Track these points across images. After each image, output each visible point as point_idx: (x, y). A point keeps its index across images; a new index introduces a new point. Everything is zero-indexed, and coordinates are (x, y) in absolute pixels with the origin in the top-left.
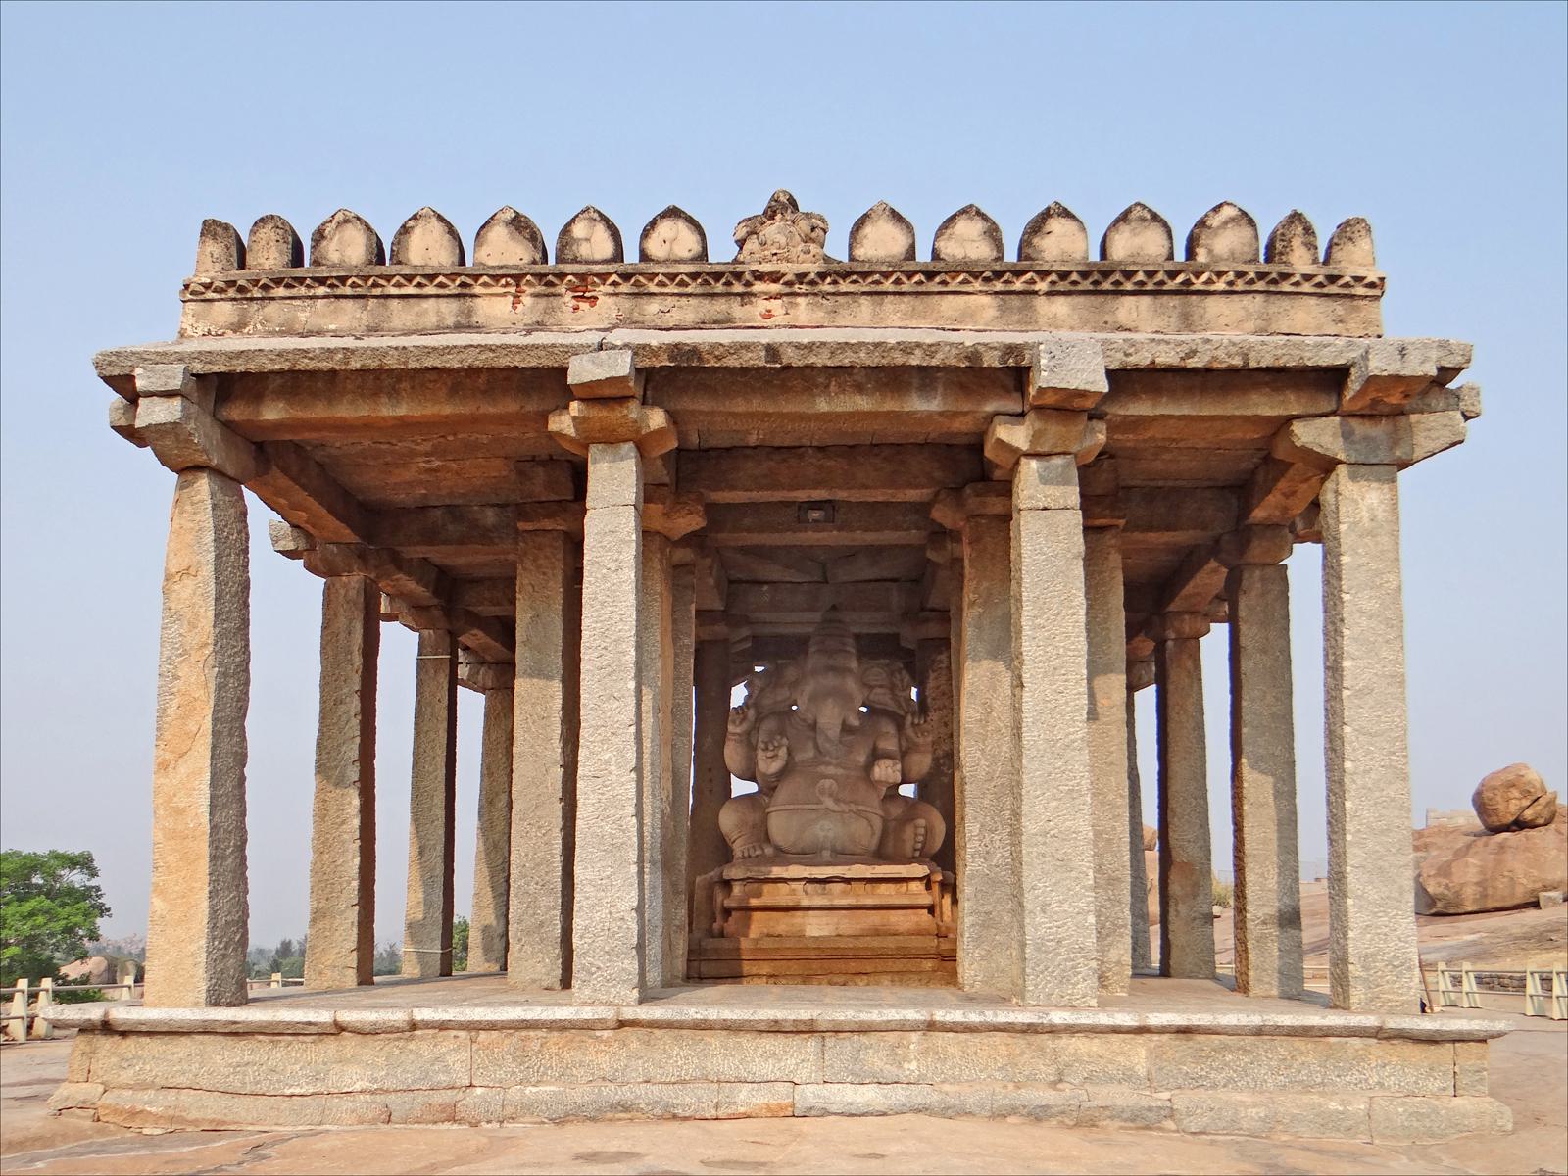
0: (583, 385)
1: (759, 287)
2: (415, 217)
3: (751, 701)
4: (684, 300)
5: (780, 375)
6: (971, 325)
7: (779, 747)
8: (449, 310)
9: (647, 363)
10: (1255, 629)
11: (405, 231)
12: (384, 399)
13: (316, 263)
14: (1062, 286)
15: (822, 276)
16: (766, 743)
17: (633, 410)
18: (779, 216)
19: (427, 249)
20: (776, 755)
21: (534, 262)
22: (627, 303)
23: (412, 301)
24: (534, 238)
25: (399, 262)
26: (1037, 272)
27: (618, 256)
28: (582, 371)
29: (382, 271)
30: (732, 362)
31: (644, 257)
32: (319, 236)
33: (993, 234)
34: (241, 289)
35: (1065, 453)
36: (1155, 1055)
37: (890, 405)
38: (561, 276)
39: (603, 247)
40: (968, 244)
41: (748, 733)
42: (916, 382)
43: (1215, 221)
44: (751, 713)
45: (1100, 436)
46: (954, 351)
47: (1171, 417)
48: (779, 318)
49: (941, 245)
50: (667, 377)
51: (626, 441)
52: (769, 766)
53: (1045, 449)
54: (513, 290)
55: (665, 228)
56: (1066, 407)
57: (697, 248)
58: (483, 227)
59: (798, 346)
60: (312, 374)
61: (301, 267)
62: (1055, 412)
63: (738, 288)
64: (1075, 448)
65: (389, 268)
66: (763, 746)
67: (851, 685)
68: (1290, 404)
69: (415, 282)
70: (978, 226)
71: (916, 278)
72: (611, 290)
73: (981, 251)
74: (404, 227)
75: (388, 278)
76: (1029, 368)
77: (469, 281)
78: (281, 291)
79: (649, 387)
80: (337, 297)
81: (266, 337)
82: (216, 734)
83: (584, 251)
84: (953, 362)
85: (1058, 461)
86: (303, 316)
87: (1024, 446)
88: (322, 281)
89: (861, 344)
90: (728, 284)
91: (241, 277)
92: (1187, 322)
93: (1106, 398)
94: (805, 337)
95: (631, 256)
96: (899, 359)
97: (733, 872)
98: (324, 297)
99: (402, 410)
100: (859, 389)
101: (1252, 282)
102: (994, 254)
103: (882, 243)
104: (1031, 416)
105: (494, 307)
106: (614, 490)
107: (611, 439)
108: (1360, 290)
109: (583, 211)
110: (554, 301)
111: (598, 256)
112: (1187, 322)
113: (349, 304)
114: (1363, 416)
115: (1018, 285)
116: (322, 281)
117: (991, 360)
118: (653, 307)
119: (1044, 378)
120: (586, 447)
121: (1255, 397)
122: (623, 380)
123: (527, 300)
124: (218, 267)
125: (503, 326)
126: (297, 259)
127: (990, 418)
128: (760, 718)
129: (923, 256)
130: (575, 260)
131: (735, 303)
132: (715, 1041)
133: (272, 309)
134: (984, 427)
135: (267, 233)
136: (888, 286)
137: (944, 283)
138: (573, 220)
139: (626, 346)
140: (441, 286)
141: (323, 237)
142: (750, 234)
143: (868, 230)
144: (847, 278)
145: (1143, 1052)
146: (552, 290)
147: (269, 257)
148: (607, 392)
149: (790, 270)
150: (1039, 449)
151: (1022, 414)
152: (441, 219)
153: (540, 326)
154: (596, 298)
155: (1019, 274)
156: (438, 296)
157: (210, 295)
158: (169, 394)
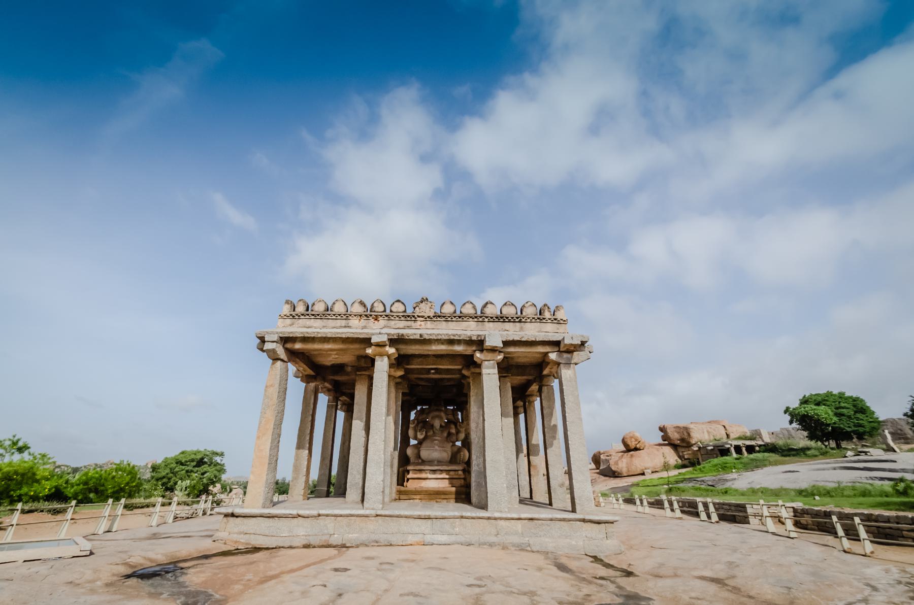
5: (423, 341)
6: (470, 330)
8: (343, 323)
17: (387, 348)
19: (339, 308)
27: (385, 311)
28: (374, 340)
29: (328, 313)
30: (411, 337)
31: (391, 311)
32: (314, 304)
33: (474, 307)
39: (381, 308)
40: (468, 310)
45: (500, 357)
48: (423, 326)
50: (394, 341)
52: (420, 436)
55: (396, 304)
56: (493, 350)
60: (308, 338)
61: (309, 312)
65: (329, 312)
73: (472, 311)
81: (299, 328)
83: (377, 309)
91: (294, 314)
92: (521, 329)
94: (429, 332)
96: (452, 337)
97: (409, 468)
100: (443, 344)
103: (448, 309)
105: (354, 322)
106: (382, 367)
107: (381, 355)
117: (474, 338)
118: (392, 323)
119: (489, 343)
126: (307, 310)
128: (418, 423)
129: (458, 313)
132: (402, 520)
135: (301, 303)
147: (300, 309)
153: (365, 327)
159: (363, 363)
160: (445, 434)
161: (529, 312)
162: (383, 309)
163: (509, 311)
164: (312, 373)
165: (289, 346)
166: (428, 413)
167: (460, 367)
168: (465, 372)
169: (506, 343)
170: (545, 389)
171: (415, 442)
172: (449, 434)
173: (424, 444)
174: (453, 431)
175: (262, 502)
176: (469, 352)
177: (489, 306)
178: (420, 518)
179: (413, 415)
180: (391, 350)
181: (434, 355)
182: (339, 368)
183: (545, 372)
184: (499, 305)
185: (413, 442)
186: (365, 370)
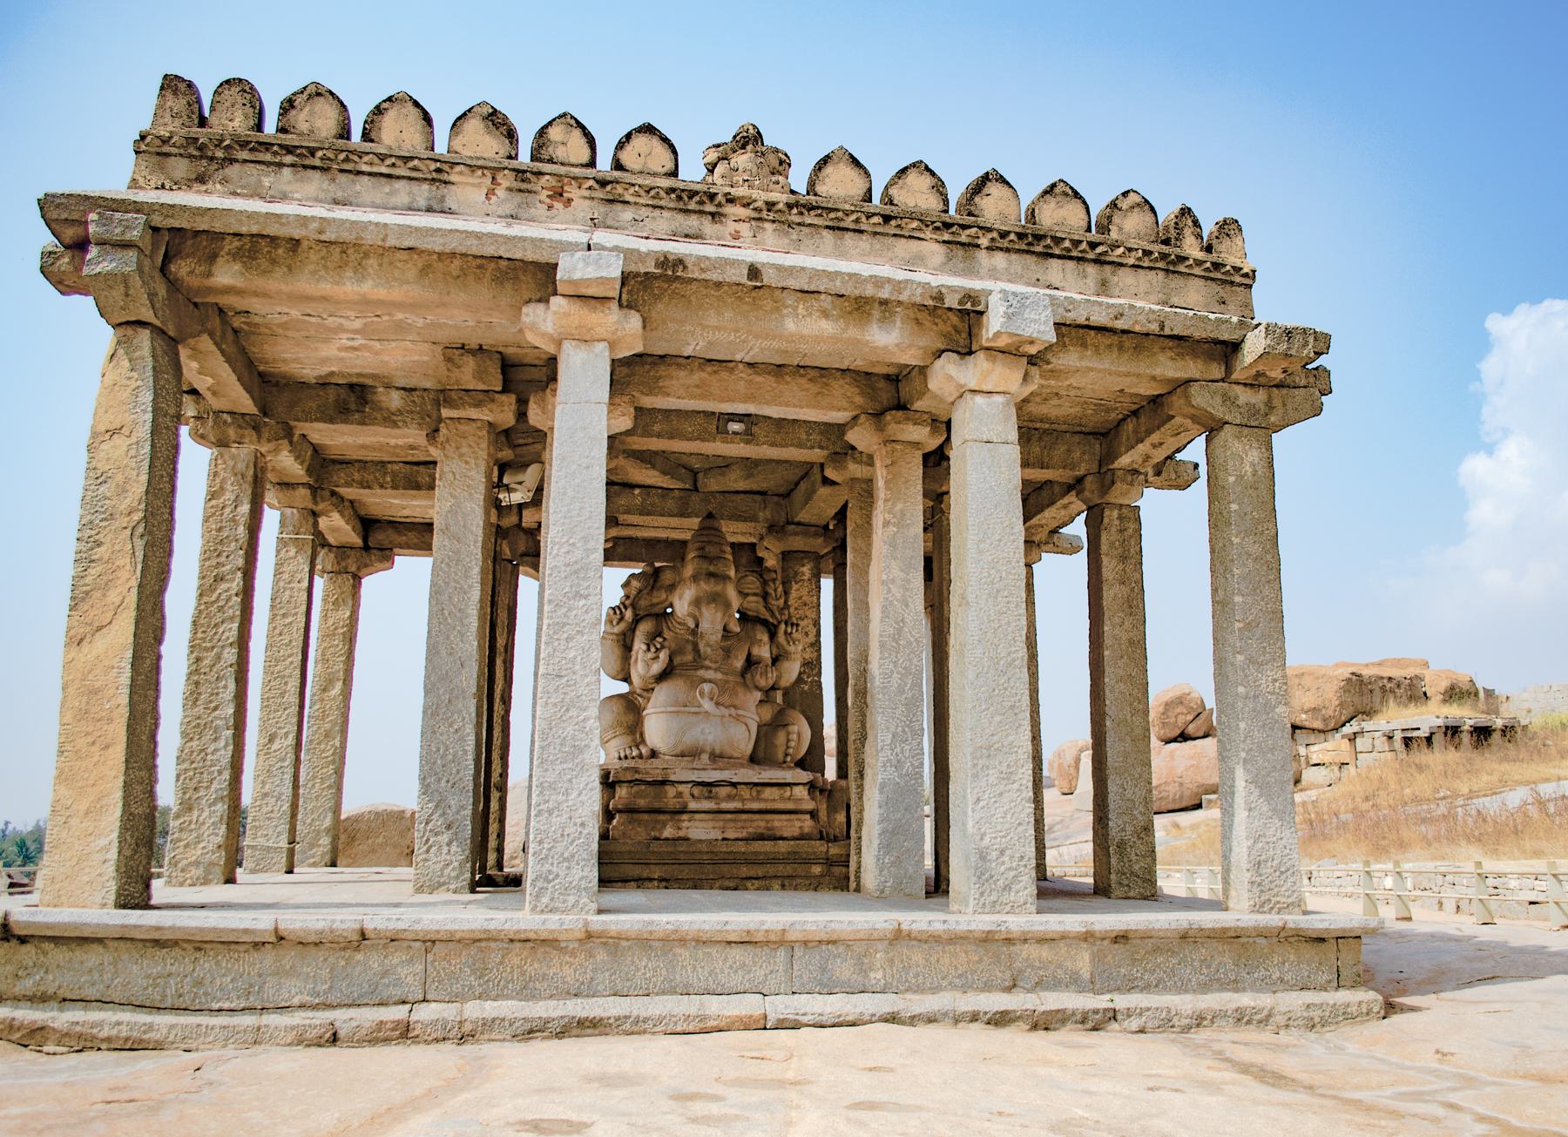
0: (571, 282)
1: (729, 209)
2: (390, 99)
4: (657, 212)
7: (663, 647)
8: (423, 192)
9: (633, 268)
10: (1114, 562)
11: (378, 111)
12: (349, 274)
13: (282, 130)
14: (1005, 243)
15: (790, 206)
18: (749, 147)
21: (510, 157)
22: (599, 211)
23: (383, 180)
24: (511, 135)
25: (372, 141)
26: (981, 228)
27: (592, 164)
30: (714, 276)
31: (618, 165)
32: (288, 105)
34: (201, 148)
36: (1097, 958)
37: (853, 332)
38: (540, 174)
39: (576, 150)
40: (915, 195)
41: (624, 634)
42: (876, 313)
43: (1124, 204)
44: (629, 614)
46: (919, 290)
47: (1092, 369)
49: (893, 191)
50: (644, 287)
53: (989, 388)
54: (488, 181)
55: (640, 142)
57: (670, 166)
58: (459, 118)
59: (779, 268)
63: (710, 208)
66: (644, 647)
68: (1191, 368)
69: (389, 161)
70: (927, 180)
71: (876, 220)
72: (587, 193)
73: (930, 203)
74: (377, 107)
75: (361, 155)
76: (981, 313)
77: (446, 167)
78: (244, 155)
79: (625, 290)
80: (305, 167)
82: (139, 608)
83: (560, 153)
84: (918, 300)
85: (999, 399)
86: (266, 182)
87: (973, 385)
88: (289, 150)
89: (837, 273)
90: (701, 203)
91: (202, 134)
93: (1050, 348)
95: (604, 163)
96: (869, 291)
98: (293, 165)
99: (367, 288)
100: (825, 314)
101: (1156, 260)
102: (941, 207)
104: (981, 355)
107: (585, 340)
108: (1238, 279)
109: (560, 117)
110: (530, 197)
111: (573, 161)
112: (1104, 287)
113: (317, 175)
114: (1245, 385)
115: (963, 239)
116: (289, 150)
117: (952, 301)
118: (627, 214)
120: (559, 344)
121: (1162, 358)
122: (614, 279)
123: (500, 192)
124: (178, 122)
125: (478, 218)
126: (259, 127)
128: (637, 620)
130: (551, 161)
131: (707, 220)
133: (233, 171)
135: (232, 93)
136: (848, 222)
137: (898, 226)
138: (550, 123)
139: (616, 248)
140: (415, 169)
141: (293, 107)
142: (719, 159)
143: (829, 170)
144: (807, 213)
145: (1087, 956)
146: (524, 186)
148: (589, 292)
149: (761, 197)
150: (985, 388)
151: (970, 353)
152: (416, 104)
154: (570, 201)
155: (964, 227)
156: (410, 179)
157: (166, 149)
158: (126, 245)
159: (467, 375)
160: (739, 663)
161: (1131, 226)
162: (585, 156)
163: (1059, 218)
164: (247, 404)
165: (182, 269)
166: (672, 588)
169: (1071, 331)
170: (1111, 515)
172: (750, 662)
173: (662, 693)
174: (764, 652)
175: (113, 887)
176: (910, 358)
177: (994, 189)
180: (634, 321)
181: (750, 365)
182: (353, 398)
183: (1125, 461)
184: (1028, 192)
186: (478, 404)
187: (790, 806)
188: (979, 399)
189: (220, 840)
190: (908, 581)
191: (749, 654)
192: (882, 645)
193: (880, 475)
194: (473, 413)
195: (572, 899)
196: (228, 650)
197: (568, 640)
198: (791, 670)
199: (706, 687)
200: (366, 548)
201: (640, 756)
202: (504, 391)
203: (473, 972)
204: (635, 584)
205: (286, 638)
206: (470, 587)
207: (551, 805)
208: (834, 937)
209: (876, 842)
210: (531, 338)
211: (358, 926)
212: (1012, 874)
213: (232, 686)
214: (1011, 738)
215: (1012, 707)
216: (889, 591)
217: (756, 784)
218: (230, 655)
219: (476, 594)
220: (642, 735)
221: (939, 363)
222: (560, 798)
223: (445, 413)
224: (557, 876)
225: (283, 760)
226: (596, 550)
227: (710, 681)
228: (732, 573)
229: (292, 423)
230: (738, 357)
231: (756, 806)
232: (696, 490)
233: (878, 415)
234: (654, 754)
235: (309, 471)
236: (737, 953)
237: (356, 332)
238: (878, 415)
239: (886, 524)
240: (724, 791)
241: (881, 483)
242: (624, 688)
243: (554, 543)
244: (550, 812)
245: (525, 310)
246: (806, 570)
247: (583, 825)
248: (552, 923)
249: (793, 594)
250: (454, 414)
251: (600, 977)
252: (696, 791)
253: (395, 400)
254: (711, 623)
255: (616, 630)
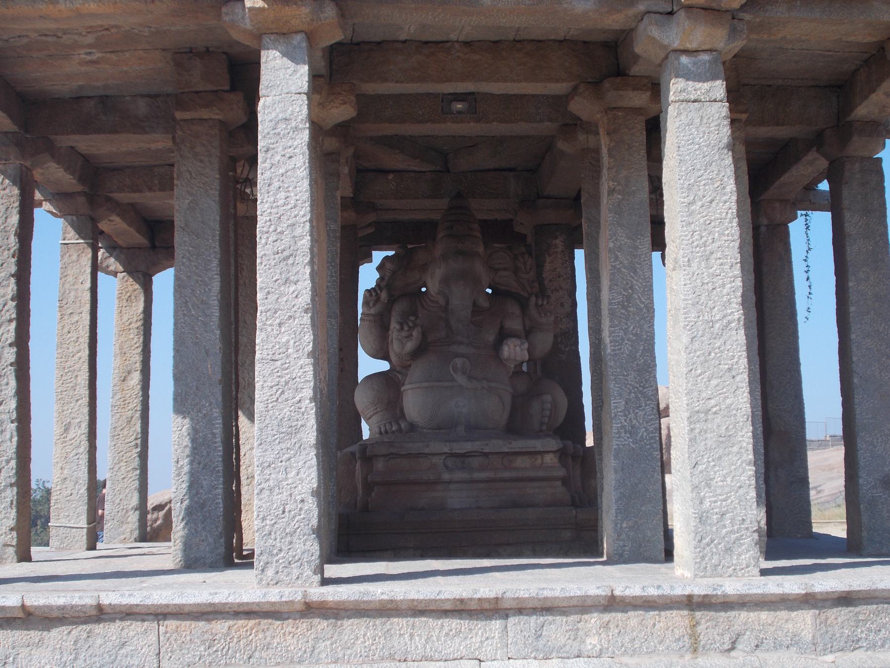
3: (383, 284)
7: (415, 326)
16: (401, 324)
20: (412, 335)
35: (711, 50)
44: (384, 295)
51: (297, 32)
62: (703, 11)
64: (720, 45)
66: (398, 327)
67: (479, 268)
85: (705, 57)
87: (676, 45)
104: (681, 15)
120: (259, 37)
127: (641, 17)
128: (393, 300)
134: (633, 25)
150: (689, 46)
151: (671, 13)
160: (491, 337)
166: (424, 268)
167: (559, 88)
168: (581, 107)
171: (383, 366)
173: (417, 370)
178: (462, 610)
179: (368, 276)
181: (467, 44)
185: (369, 365)
187: (541, 474)
188: (684, 59)
189: (12, 523)
190: (636, 248)
191: (502, 328)
192: (612, 313)
193: (604, 142)
194: (205, 114)
195: (296, 572)
196: (7, 349)
197: (280, 325)
198: (544, 341)
199: (459, 362)
200: (153, 247)
201: (400, 430)
202: (233, 89)
203: (203, 642)
204: (388, 265)
205: (74, 335)
206: (211, 279)
207: (271, 483)
208: (548, 604)
209: (614, 507)
210: (236, 36)
211: (94, 603)
212: (733, 537)
213: (13, 383)
214: (728, 401)
215: (730, 370)
216: (617, 258)
217: (507, 454)
218: (10, 355)
219: (216, 286)
220: (402, 410)
221: (642, 26)
222: (280, 476)
223: (179, 115)
224: (281, 550)
225: (78, 447)
226: (302, 237)
227: (463, 356)
228: (481, 249)
229: (52, 137)
230: (453, 37)
231: (506, 474)
232: (448, 171)
233: (596, 84)
234: (413, 427)
235: (81, 180)
236: (453, 624)
237: (90, 46)
238: (596, 84)
239: (611, 192)
240: (475, 462)
241: (604, 151)
242: (383, 366)
243: (262, 232)
244: (271, 490)
245: (224, 10)
246: (559, 243)
247: (302, 501)
248: (274, 595)
249: (548, 266)
250: (187, 115)
251: (321, 645)
252: (450, 462)
253: (142, 107)
254: (460, 299)
255: (372, 311)
